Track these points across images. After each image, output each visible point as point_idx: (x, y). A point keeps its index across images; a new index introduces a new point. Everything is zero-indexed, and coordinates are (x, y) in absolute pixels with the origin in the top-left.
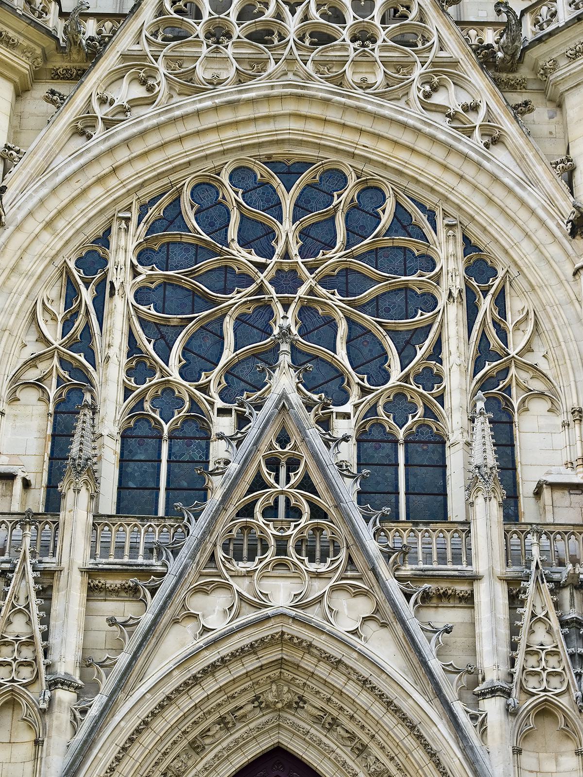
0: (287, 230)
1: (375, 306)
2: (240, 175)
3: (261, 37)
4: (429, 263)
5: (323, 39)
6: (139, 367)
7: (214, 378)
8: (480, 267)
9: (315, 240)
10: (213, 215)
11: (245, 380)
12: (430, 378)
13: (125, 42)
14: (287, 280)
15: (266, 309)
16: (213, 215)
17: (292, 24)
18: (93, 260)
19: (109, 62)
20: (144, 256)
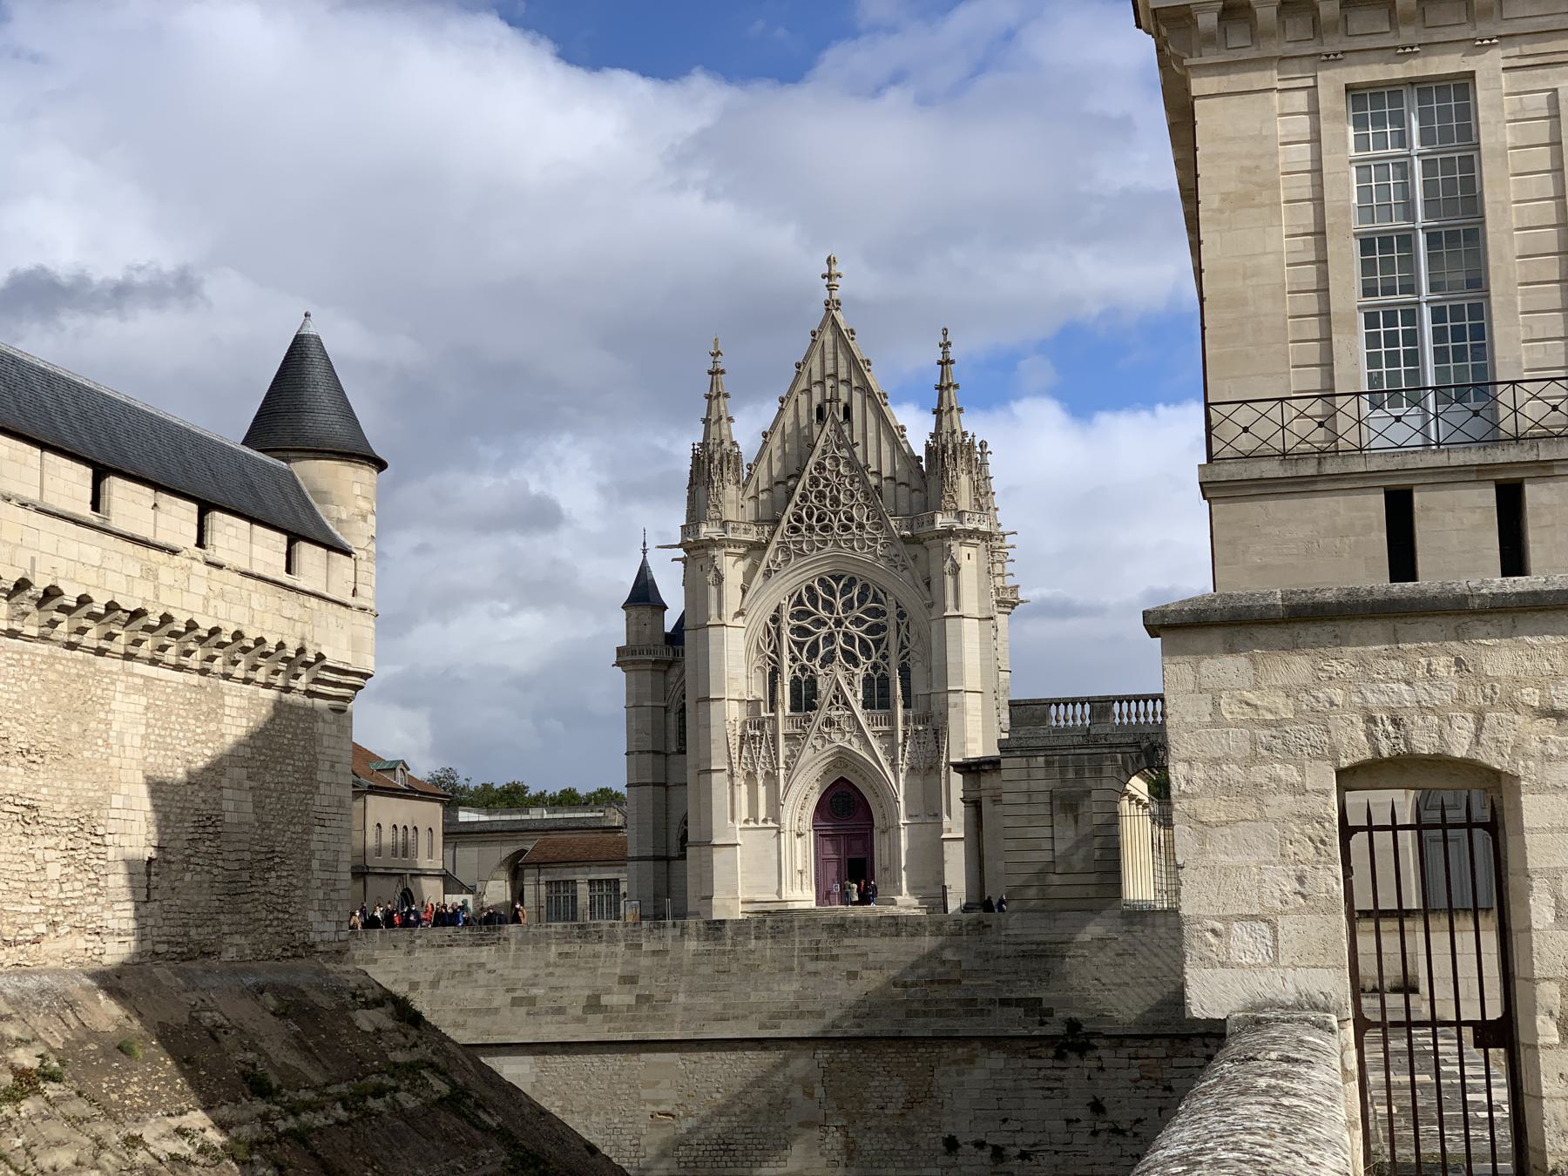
0: (839, 603)
1: (867, 632)
2: (822, 581)
3: (824, 528)
4: (884, 613)
5: (846, 528)
6: (794, 659)
7: (818, 661)
8: (902, 615)
9: (848, 605)
10: (814, 600)
11: (828, 659)
12: (884, 657)
13: (778, 538)
14: (839, 623)
15: (831, 635)
16: (814, 600)
17: (836, 524)
18: (775, 620)
19: (773, 545)
20: (792, 616)
